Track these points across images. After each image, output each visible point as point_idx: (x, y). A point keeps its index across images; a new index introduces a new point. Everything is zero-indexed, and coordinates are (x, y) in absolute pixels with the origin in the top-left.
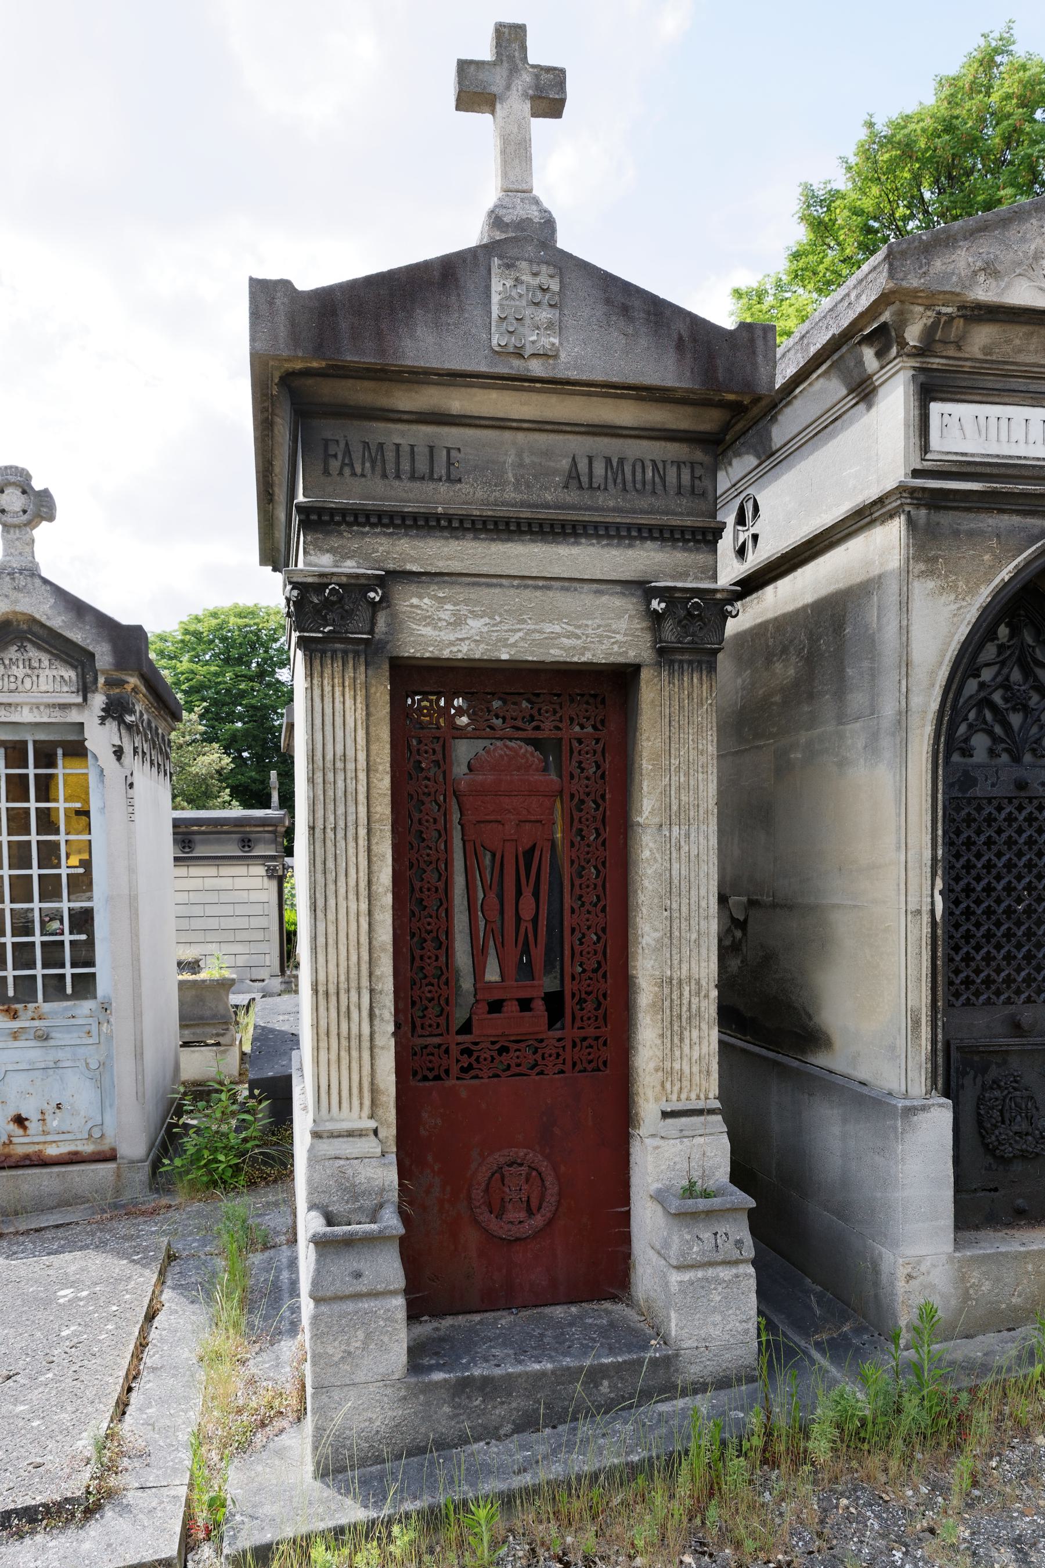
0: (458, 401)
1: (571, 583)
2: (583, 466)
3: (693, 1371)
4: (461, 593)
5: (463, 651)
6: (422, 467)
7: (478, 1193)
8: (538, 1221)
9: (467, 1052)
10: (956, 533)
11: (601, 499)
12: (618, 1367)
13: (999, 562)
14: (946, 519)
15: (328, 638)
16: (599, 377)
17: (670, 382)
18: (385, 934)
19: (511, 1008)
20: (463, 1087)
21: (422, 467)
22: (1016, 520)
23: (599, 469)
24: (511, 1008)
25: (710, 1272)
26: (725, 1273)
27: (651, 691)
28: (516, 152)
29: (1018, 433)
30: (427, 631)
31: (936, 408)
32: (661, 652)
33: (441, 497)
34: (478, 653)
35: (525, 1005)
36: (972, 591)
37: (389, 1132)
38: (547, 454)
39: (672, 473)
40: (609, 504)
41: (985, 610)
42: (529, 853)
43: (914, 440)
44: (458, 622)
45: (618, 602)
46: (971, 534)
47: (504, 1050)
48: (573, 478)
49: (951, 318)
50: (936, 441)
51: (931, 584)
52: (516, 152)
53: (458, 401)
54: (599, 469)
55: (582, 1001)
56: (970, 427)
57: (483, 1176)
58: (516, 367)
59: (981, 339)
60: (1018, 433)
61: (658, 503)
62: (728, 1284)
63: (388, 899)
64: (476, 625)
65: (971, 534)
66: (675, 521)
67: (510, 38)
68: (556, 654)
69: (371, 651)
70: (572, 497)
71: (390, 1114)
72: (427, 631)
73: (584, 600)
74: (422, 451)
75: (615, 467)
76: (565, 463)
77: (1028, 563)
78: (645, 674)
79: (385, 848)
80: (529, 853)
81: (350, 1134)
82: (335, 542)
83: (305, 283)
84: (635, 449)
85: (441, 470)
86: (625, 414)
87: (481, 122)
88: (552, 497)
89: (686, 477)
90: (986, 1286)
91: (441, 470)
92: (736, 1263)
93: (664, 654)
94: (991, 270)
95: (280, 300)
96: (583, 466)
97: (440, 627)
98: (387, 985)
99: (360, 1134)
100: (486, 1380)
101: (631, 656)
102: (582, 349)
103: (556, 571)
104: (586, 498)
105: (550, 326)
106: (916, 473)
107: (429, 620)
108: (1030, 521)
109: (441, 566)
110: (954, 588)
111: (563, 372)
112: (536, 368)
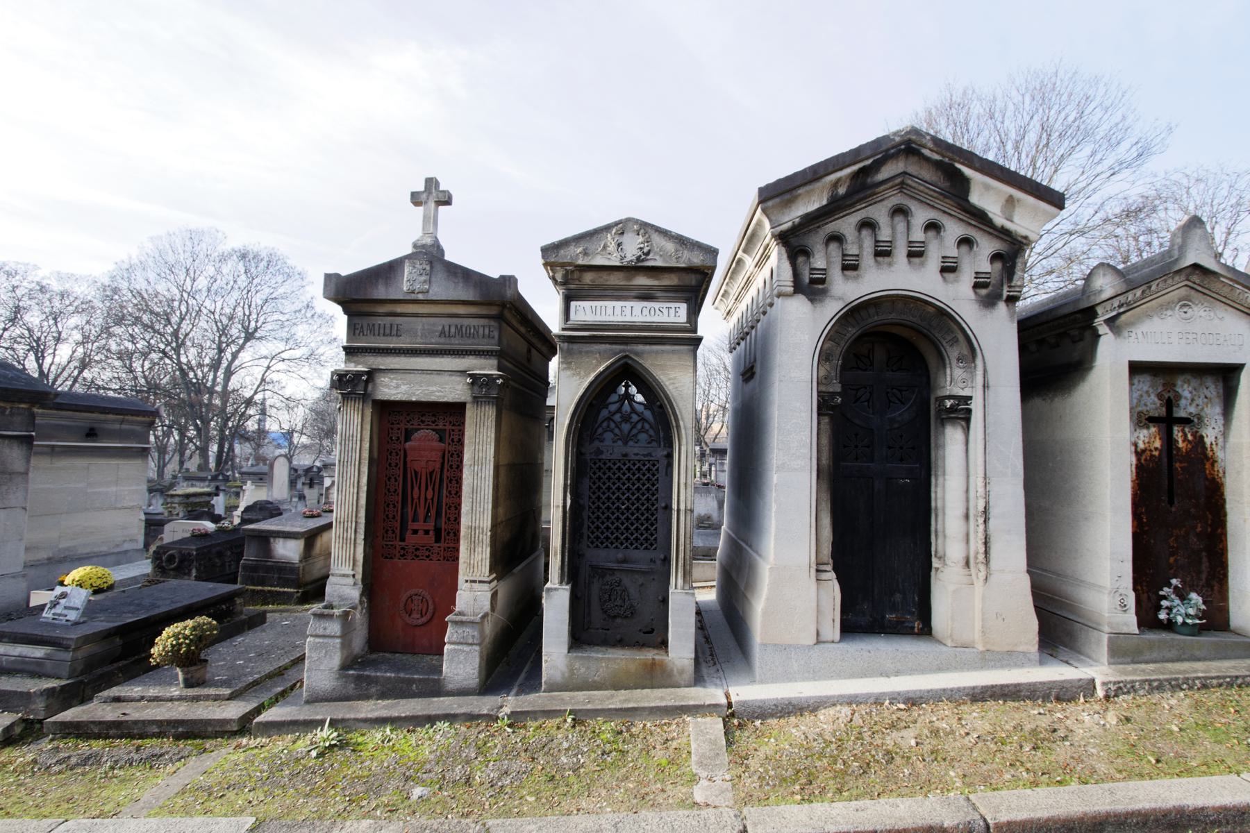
0: (399, 309)
1: (440, 372)
2: (447, 329)
3: (450, 687)
4: (399, 376)
5: (398, 397)
6: (388, 331)
7: (402, 605)
8: (424, 619)
9: (403, 549)
10: (580, 352)
11: (453, 340)
12: (420, 680)
13: (599, 364)
14: (576, 347)
15: (349, 393)
16: (456, 298)
17: (471, 298)
18: (363, 501)
19: (421, 533)
20: (400, 563)
21: (388, 331)
22: (608, 346)
23: (453, 330)
24: (421, 533)
25: (460, 647)
26: (466, 648)
27: (470, 413)
28: (431, 222)
29: (610, 311)
30: (386, 390)
31: (573, 304)
32: (475, 397)
33: (393, 343)
34: (404, 398)
35: (427, 532)
36: (587, 375)
37: (359, 577)
38: (434, 325)
39: (481, 330)
40: (456, 344)
41: (591, 384)
42: (431, 473)
43: (562, 316)
44: (397, 387)
45: (458, 379)
46: (587, 352)
47: (417, 549)
48: (442, 333)
49: (572, 272)
50: (572, 316)
51: (568, 373)
52: (431, 222)
53: (399, 309)
54: (453, 330)
55: (448, 534)
56: (588, 311)
57: (404, 599)
58: (413, 297)
59: (588, 278)
60: (610, 311)
61: (476, 341)
62: (467, 653)
63: (365, 488)
64: (404, 388)
65: (587, 352)
66: (480, 347)
67: (431, 183)
68: (433, 398)
69: (365, 397)
70: (442, 340)
71: (360, 569)
72: (386, 390)
73: (446, 378)
74: (388, 326)
75: (459, 329)
76: (440, 328)
77: (612, 364)
78: (468, 406)
79: (365, 470)
80: (431, 473)
81: (344, 575)
82: (355, 359)
83: (344, 274)
84: (466, 322)
85: (394, 332)
86: (461, 310)
87: (420, 210)
88: (435, 342)
89: (487, 331)
90: (583, 670)
91: (394, 332)
92: (472, 644)
93: (476, 400)
94: (585, 253)
95: (334, 280)
96: (447, 329)
97: (392, 389)
98: (362, 520)
99: (347, 576)
100: (368, 676)
101: (463, 399)
102: (441, 289)
103: (434, 368)
104: (448, 341)
105: (425, 282)
106: (564, 329)
107: (387, 386)
108: (614, 347)
109: (392, 366)
110: (579, 374)
111: (431, 297)
112: (421, 297)
